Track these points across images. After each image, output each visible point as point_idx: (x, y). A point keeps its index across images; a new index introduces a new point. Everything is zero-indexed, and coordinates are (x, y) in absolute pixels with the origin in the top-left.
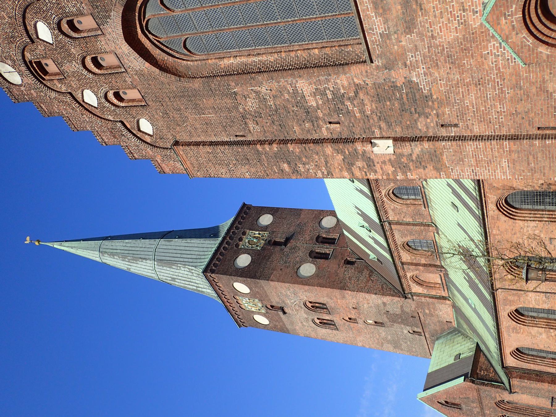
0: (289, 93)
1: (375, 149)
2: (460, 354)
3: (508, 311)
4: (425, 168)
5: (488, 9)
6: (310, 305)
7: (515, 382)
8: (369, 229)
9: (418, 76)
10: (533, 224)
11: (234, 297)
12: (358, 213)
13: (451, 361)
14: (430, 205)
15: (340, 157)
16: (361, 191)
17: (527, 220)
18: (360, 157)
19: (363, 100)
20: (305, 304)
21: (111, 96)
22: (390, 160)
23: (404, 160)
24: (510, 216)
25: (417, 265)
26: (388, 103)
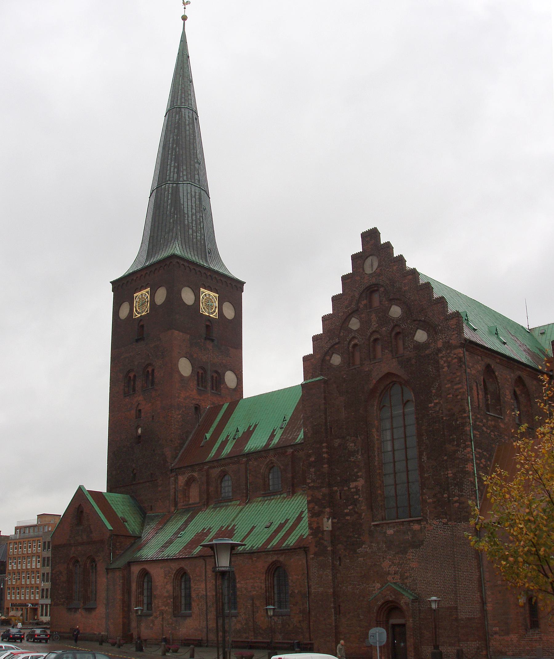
0: (357, 472)
1: (325, 520)
2: (127, 522)
3: (185, 568)
4: (316, 546)
5: (393, 586)
6: (150, 369)
7: (118, 574)
8: (236, 437)
9: (365, 548)
10: (263, 586)
11: (148, 284)
12: (250, 427)
13: (120, 515)
14: (266, 498)
15: (320, 497)
16: (272, 436)
17: (266, 582)
18: (321, 509)
19: (353, 516)
20: (150, 364)
21: (356, 341)
22: (320, 527)
23: (320, 535)
24: (268, 571)
25: (208, 484)
26: (351, 530)
